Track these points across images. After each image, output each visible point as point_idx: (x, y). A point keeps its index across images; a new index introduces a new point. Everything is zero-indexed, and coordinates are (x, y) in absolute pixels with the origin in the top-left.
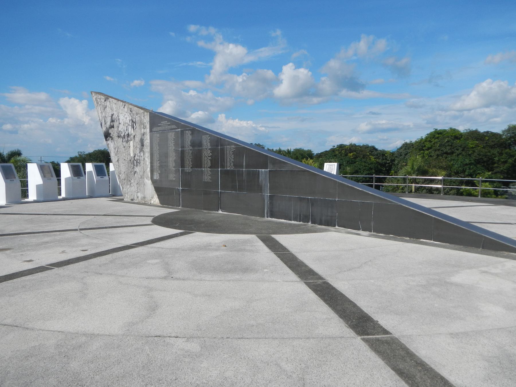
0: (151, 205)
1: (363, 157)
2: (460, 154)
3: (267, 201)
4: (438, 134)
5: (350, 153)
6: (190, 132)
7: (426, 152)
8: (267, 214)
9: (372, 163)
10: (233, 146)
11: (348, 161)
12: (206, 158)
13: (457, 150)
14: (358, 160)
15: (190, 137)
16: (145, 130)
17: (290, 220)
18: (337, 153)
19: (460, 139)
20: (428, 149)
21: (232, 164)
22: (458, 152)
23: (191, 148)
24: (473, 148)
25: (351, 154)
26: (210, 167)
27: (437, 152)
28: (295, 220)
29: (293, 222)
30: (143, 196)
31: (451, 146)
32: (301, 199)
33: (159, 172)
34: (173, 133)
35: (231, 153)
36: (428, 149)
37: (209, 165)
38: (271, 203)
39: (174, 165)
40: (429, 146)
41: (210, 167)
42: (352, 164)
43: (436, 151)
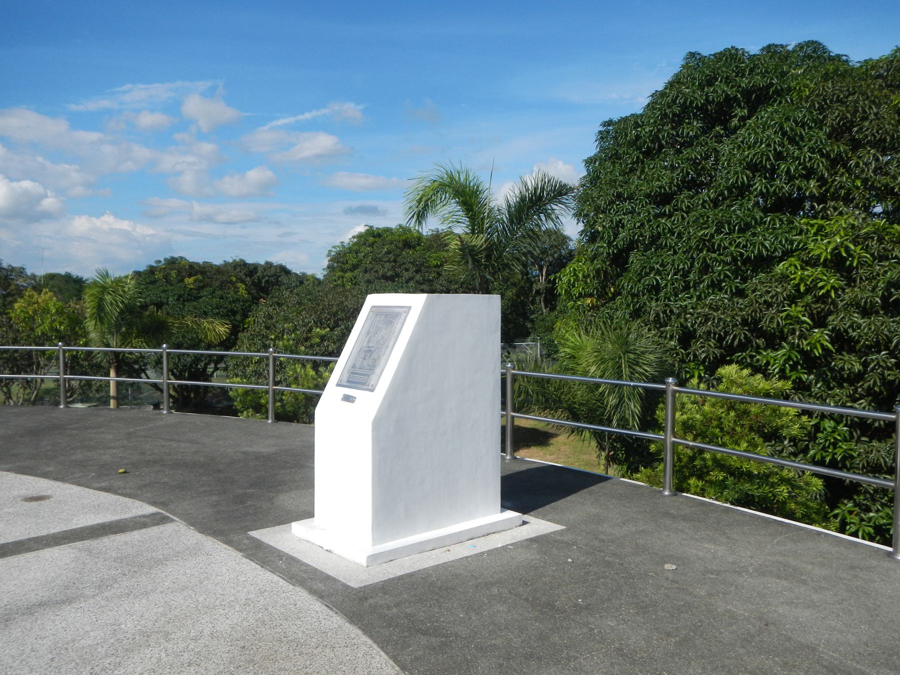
1: (221, 287)
2: (411, 279)
4: (374, 237)
5: (190, 276)
7: (349, 275)
9: (238, 300)
11: (180, 296)
13: (407, 270)
14: (204, 292)
18: (158, 276)
19: (414, 248)
20: (355, 267)
22: (406, 275)
24: (437, 266)
25: (192, 280)
27: (367, 276)
31: (395, 261)
36: (355, 267)
40: (355, 261)
42: (188, 301)
43: (366, 272)
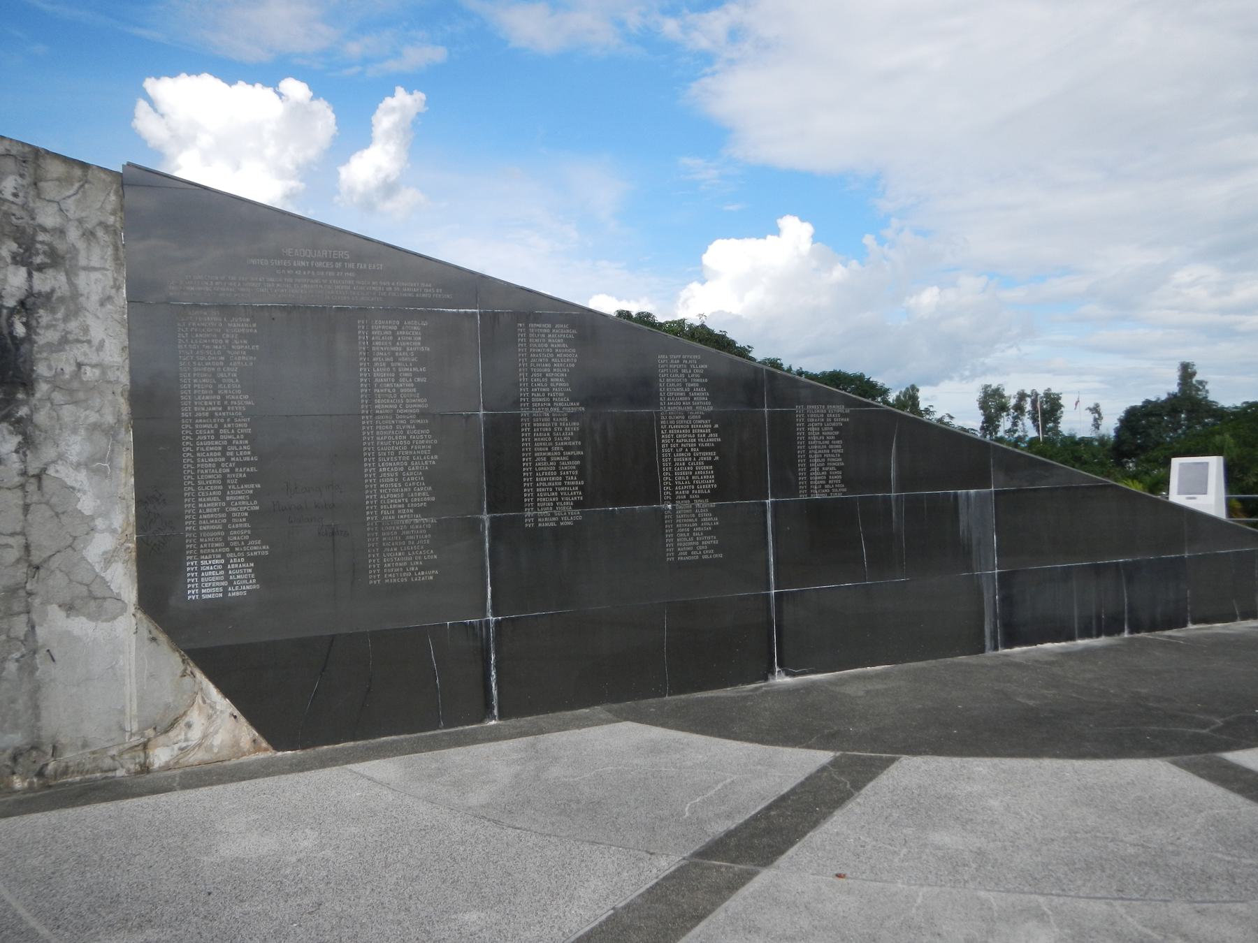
0: (145, 782)
3: (991, 597)
6: (564, 331)
8: (994, 637)
10: (841, 408)
12: (681, 457)
15: (570, 357)
16: (43, 282)
17: (1071, 638)
21: (837, 476)
23: (575, 408)
26: (713, 495)
28: (1086, 634)
29: (1081, 643)
30: (17, 739)
32: (1098, 570)
33: (259, 549)
34: (415, 326)
35: (831, 434)
37: (708, 481)
38: (1007, 600)
39: (423, 495)
41: (713, 495)
